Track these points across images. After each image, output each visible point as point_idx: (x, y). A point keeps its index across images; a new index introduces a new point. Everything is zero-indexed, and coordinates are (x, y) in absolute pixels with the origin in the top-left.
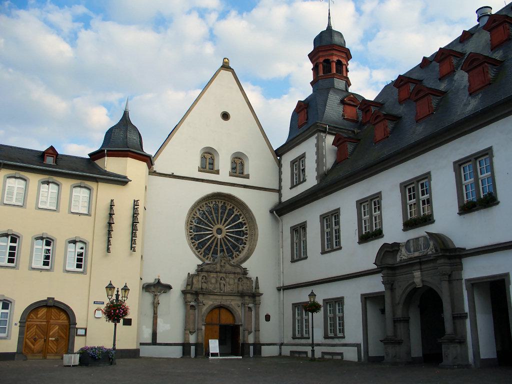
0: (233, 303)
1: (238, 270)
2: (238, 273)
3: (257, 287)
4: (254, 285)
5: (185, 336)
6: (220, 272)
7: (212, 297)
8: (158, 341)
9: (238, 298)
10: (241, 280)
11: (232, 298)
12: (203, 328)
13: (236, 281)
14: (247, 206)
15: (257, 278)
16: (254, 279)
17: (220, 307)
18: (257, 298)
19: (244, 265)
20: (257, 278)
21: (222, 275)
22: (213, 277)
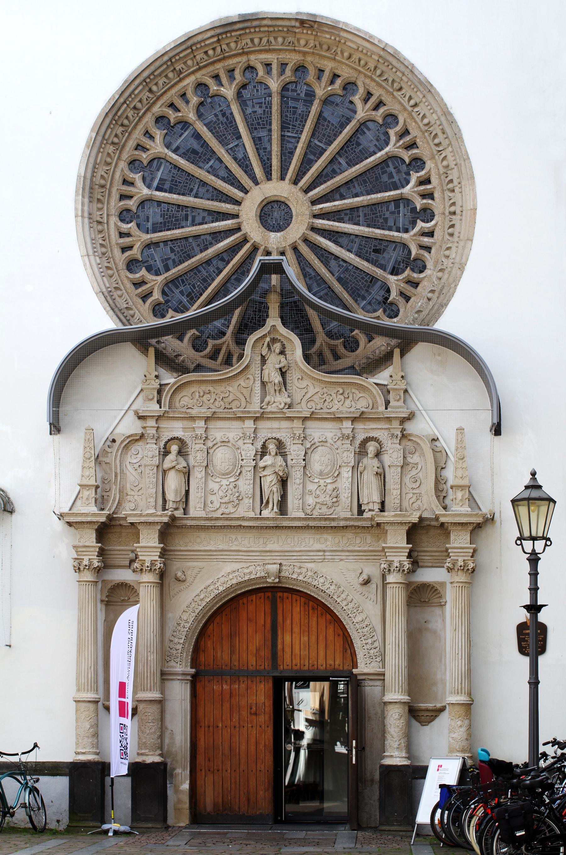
10: (372, 448)
14: (411, 69)
15: (460, 430)
22: (225, 442)
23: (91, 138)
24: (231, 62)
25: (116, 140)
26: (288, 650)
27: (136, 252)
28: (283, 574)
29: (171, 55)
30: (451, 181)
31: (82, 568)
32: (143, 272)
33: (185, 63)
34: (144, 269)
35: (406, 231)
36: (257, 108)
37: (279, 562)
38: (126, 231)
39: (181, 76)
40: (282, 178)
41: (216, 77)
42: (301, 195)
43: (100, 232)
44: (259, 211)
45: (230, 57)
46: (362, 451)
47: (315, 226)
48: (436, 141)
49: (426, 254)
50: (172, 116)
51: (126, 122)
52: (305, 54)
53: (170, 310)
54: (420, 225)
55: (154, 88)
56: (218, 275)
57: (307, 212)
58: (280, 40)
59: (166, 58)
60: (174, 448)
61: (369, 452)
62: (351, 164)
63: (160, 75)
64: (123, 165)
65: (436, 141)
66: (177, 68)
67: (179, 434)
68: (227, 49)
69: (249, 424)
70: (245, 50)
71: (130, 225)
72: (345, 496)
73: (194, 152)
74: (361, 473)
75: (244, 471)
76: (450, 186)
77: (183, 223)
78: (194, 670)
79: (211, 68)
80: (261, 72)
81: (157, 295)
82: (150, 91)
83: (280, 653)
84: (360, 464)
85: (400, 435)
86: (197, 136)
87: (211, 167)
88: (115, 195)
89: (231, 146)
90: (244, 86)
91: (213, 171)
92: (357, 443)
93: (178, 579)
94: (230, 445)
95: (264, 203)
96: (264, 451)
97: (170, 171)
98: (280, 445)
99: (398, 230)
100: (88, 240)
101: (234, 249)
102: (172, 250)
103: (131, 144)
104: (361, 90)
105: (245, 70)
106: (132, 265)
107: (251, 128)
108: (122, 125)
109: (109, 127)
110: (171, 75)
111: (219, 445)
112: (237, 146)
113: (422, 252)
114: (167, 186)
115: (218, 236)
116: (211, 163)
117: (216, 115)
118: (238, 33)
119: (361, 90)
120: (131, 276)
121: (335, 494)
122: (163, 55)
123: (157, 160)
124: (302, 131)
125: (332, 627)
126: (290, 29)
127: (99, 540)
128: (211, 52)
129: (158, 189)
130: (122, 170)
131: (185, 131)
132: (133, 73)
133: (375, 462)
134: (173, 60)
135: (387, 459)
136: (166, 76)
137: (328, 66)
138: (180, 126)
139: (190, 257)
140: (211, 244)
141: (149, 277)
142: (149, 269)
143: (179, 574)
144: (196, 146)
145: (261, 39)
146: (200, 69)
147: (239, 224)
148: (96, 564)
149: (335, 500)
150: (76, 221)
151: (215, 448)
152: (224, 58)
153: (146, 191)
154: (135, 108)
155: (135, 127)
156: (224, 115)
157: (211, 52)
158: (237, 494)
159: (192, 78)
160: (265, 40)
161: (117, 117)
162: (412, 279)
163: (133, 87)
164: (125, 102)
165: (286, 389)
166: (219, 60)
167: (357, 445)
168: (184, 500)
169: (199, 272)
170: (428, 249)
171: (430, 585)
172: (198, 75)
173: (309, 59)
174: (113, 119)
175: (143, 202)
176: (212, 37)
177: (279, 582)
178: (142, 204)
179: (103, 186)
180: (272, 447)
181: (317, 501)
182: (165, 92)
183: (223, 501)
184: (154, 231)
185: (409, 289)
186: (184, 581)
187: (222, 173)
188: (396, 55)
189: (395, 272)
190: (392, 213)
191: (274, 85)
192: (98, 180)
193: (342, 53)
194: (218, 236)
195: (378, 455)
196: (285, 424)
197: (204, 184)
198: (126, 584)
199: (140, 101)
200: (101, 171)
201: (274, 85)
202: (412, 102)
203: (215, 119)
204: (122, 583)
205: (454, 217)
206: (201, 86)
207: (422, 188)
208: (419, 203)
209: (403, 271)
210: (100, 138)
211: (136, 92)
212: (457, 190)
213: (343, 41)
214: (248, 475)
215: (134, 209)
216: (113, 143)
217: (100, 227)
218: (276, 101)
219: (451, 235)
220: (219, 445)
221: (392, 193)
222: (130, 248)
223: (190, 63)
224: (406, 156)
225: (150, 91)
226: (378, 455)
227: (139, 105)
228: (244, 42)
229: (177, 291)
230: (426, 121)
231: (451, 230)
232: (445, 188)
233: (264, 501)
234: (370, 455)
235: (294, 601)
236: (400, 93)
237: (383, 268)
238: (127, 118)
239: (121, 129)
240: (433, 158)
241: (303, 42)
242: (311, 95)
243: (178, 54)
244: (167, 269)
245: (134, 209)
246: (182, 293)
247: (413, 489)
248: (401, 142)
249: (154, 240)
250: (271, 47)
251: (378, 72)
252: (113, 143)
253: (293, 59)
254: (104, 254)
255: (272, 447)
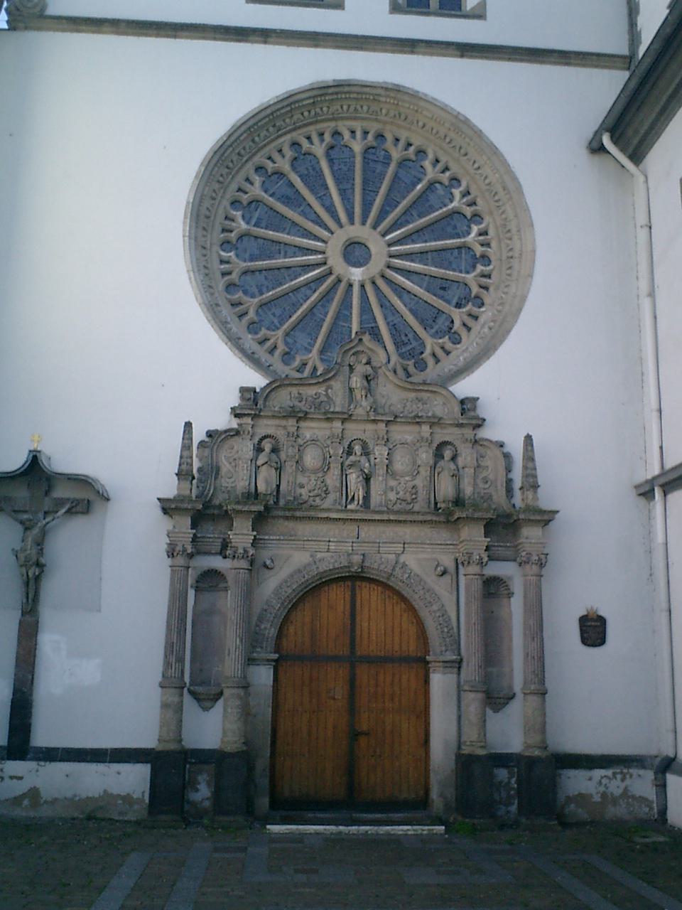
0: (412, 560)
1: (437, 407)
2: (436, 422)
3: (532, 484)
4: (517, 475)
5: (173, 712)
6: (347, 418)
7: (304, 529)
8: (42, 736)
9: (443, 535)
10: (448, 454)
11: (407, 532)
12: (263, 676)
13: (425, 456)
15: (528, 439)
16: (516, 449)
17: (354, 578)
18: (530, 534)
19: (463, 388)
20: (528, 439)
21: (354, 430)
22: (314, 441)
23: (200, 171)
24: (320, 126)
25: (221, 179)
26: (365, 636)
27: (234, 277)
28: (367, 564)
29: (273, 108)
30: (509, 231)
31: (175, 554)
32: (240, 294)
33: (284, 121)
34: (241, 292)
35: (468, 272)
36: (342, 166)
37: (363, 552)
38: (226, 259)
39: (280, 133)
40: (364, 223)
41: (309, 138)
42: (379, 237)
43: (205, 256)
44: (343, 248)
45: (322, 121)
46: (438, 455)
47: (391, 265)
48: (496, 198)
49: (485, 292)
50: (270, 166)
51: (231, 165)
52: (385, 123)
53: (263, 329)
54: (480, 268)
55: (257, 139)
56: (305, 301)
57: (385, 253)
58: (365, 108)
59: (269, 111)
60: (267, 446)
61: (445, 455)
62: (420, 216)
63: (263, 126)
64: (226, 203)
65: (496, 198)
66: (277, 125)
67: (270, 431)
68: (320, 112)
69: (338, 424)
70: (335, 116)
71: (229, 254)
72: (422, 494)
73: (287, 197)
74: (438, 474)
75: (332, 468)
76: (508, 235)
77: (277, 256)
78: (277, 655)
79: (305, 130)
80: (347, 135)
81: (252, 314)
82: (253, 141)
83: (358, 639)
84: (438, 465)
85: (473, 440)
86: (291, 185)
87: (302, 211)
88: (218, 228)
89: (319, 195)
90: (332, 147)
91: (303, 214)
92: (435, 445)
93: (266, 566)
94: (318, 443)
95: (347, 243)
96: (350, 451)
97: (267, 213)
98: (364, 446)
99: (461, 272)
100: (194, 260)
101: (320, 279)
102: (266, 278)
103: (234, 186)
104: (431, 156)
105: (333, 136)
106: (230, 287)
107: (338, 181)
108: (228, 167)
109: (216, 165)
110: (271, 129)
111: (309, 443)
112: (324, 195)
113: (482, 290)
114: (263, 224)
115: (308, 267)
116: (302, 208)
117: (307, 169)
118: (330, 97)
119: (431, 156)
120: (229, 297)
121: (414, 491)
122: (265, 108)
123: (255, 202)
124: (380, 187)
125: (406, 615)
126: (376, 97)
127: (194, 526)
128: (306, 114)
129: (254, 226)
130: (225, 208)
131: (280, 180)
132: (240, 119)
133: (452, 466)
134: (275, 115)
135: (460, 461)
136: (267, 130)
137: (404, 135)
138: (276, 176)
139: (281, 284)
140: (300, 275)
141: (245, 298)
142: (245, 292)
143: (268, 562)
144: (289, 192)
145: (349, 106)
146: (294, 129)
147: (326, 258)
148: (189, 551)
149: (414, 496)
150: (184, 241)
151: (305, 445)
152: (317, 122)
153: (243, 225)
154: (239, 154)
155: (238, 172)
156: (314, 169)
157: (306, 114)
158: (325, 489)
159: (288, 137)
160: (352, 108)
161: (223, 158)
162: (473, 313)
163: (239, 132)
164: (231, 146)
165: (371, 395)
166: (311, 124)
167: (435, 448)
168: (275, 493)
169: (290, 297)
170: (486, 288)
171: (499, 578)
172: (294, 134)
173: (388, 127)
174: (220, 158)
175: (242, 236)
176: (310, 98)
177: (362, 572)
178: (241, 237)
179: (208, 217)
180: (357, 449)
181: (398, 497)
182: (265, 145)
183: (311, 494)
184: (252, 260)
185: (470, 322)
186: (271, 569)
187: (313, 216)
188: (466, 122)
189: (458, 306)
190: (456, 258)
191: (357, 147)
192: (204, 211)
193: (418, 122)
194: (308, 267)
195: (454, 458)
196: (370, 427)
197: (295, 224)
198: (216, 571)
199: (244, 148)
200: (207, 203)
201: (357, 147)
202: (476, 166)
203: (306, 172)
204: (212, 570)
205: (512, 260)
206: (295, 144)
207: (481, 238)
208: (479, 250)
209: (465, 306)
210: (208, 173)
211: (242, 138)
212: (515, 238)
213: (420, 110)
214: (335, 471)
215: (234, 241)
216: (218, 182)
217: (204, 252)
218: (359, 160)
219: (509, 275)
220: (309, 443)
221: (455, 241)
222: (230, 273)
223: (288, 120)
224: (468, 211)
225: (253, 141)
226: (454, 458)
227: (243, 152)
228: (335, 108)
229: (269, 313)
230: (487, 181)
231: (509, 272)
232: (501, 236)
233: (350, 498)
234: (446, 458)
235: (372, 589)
236: (466, 158)
237: (448, 302)
238: (232, 161)
239: (227, 170)
240: (491, 213)
241: (384, 111)
242: (388, 158)
243: (278, 110)
244: (261, 293)
245: (234, 241)
246: (274, 315)
247: (485, 489)
248: (465, 200)
249: (252, 269)
250: (358, 115)
251: (448, 140)
252: (218, 182)
253: (374, 127)
254: (207, 275)
255: (357, 449)
